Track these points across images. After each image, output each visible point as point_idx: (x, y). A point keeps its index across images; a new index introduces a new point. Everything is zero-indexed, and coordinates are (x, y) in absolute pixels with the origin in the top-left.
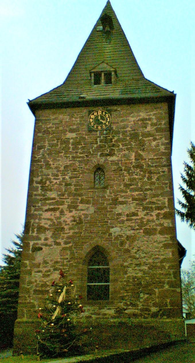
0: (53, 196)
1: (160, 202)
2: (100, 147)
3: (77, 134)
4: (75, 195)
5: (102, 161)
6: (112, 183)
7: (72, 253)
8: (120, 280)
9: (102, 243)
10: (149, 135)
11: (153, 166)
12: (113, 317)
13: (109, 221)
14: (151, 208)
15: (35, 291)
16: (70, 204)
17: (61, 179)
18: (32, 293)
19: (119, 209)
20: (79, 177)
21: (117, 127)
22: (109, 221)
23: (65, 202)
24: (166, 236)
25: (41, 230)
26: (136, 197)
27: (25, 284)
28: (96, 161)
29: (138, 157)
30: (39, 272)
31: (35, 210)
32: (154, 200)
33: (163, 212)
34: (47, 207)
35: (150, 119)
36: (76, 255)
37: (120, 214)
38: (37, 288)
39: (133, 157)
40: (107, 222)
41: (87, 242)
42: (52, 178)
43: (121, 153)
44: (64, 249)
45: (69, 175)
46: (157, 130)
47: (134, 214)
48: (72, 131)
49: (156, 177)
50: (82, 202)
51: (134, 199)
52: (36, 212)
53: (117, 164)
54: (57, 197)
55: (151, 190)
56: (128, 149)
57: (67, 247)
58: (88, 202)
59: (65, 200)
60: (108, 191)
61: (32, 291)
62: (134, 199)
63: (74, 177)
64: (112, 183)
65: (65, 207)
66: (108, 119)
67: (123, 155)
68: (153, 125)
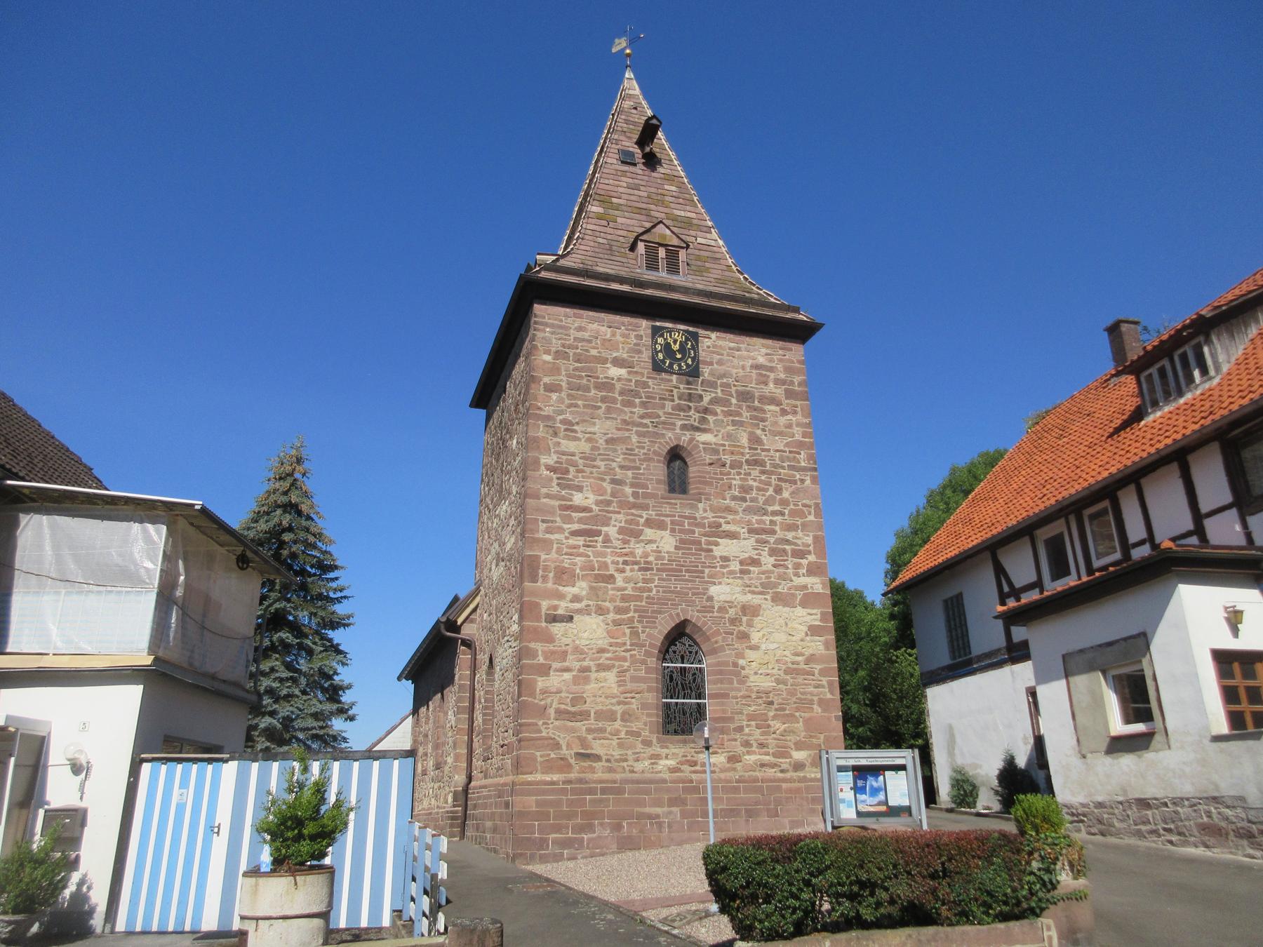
0: (585, 503)
1: (799, 542)
2: (679, 408)
3: (629, 373)
4: (634, 506)
5: (684, 440)
6: (708, 489)
7: (635, 634)
8: (732, 694)
9: (693, 615)
10: (773, 401)
11: (783, 468)
12: (722, 771)
13: (707, 571)
14: (784, 550)
15: (558, 712)
16: (623, 524)
17: (603, 469)
18: (553, 715)
19: (725, 547)
20: (640, 469)
21: (711, 374)
22: (707, 571)
23: (613, 519)
24: (814, 611)
25: (565, 577)
26: (756, 525)
27: (538, 619)
28: (672, 437)
29: (755, 440)
30: (567, 670)
31: (548, 531)
32: (790, 536)
33: (804, 562)
34: (576, 527)
35: (771, 369)
36: (643, 636)
37: (725, 559)
38: (563, 706)
39: (744, 441)
40: (703, 572)
41: (665, 612)
42: (581, 461)
43: (723, 431)
44: (617, 623)
45: (618, 460)
46: (790, 394)
47: (755, 562)
48: (618, 362)
49: (791, 490)
50: (649, 523)
51: (751, 531)
52: (548, 536)
53: (716, 452)
54: (594, 507)
55: (782, 514)
56: (734, 423)
57: (624, 620)
58: (661, 526)
59: (614, 516)
60: (701, 506)
61: (552, 711)
62: (751, 531)
63: (628, 468)
64: (708, 489)
65: (612, 531)
66: (692, 352)
67: (725, 435)
68: (778, 382)
